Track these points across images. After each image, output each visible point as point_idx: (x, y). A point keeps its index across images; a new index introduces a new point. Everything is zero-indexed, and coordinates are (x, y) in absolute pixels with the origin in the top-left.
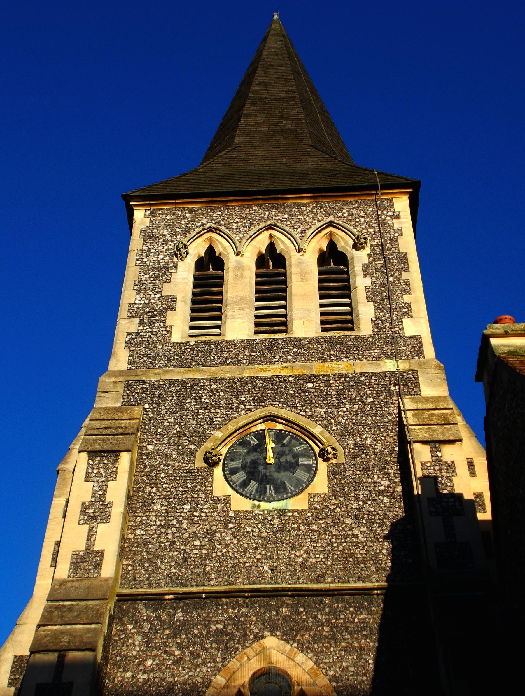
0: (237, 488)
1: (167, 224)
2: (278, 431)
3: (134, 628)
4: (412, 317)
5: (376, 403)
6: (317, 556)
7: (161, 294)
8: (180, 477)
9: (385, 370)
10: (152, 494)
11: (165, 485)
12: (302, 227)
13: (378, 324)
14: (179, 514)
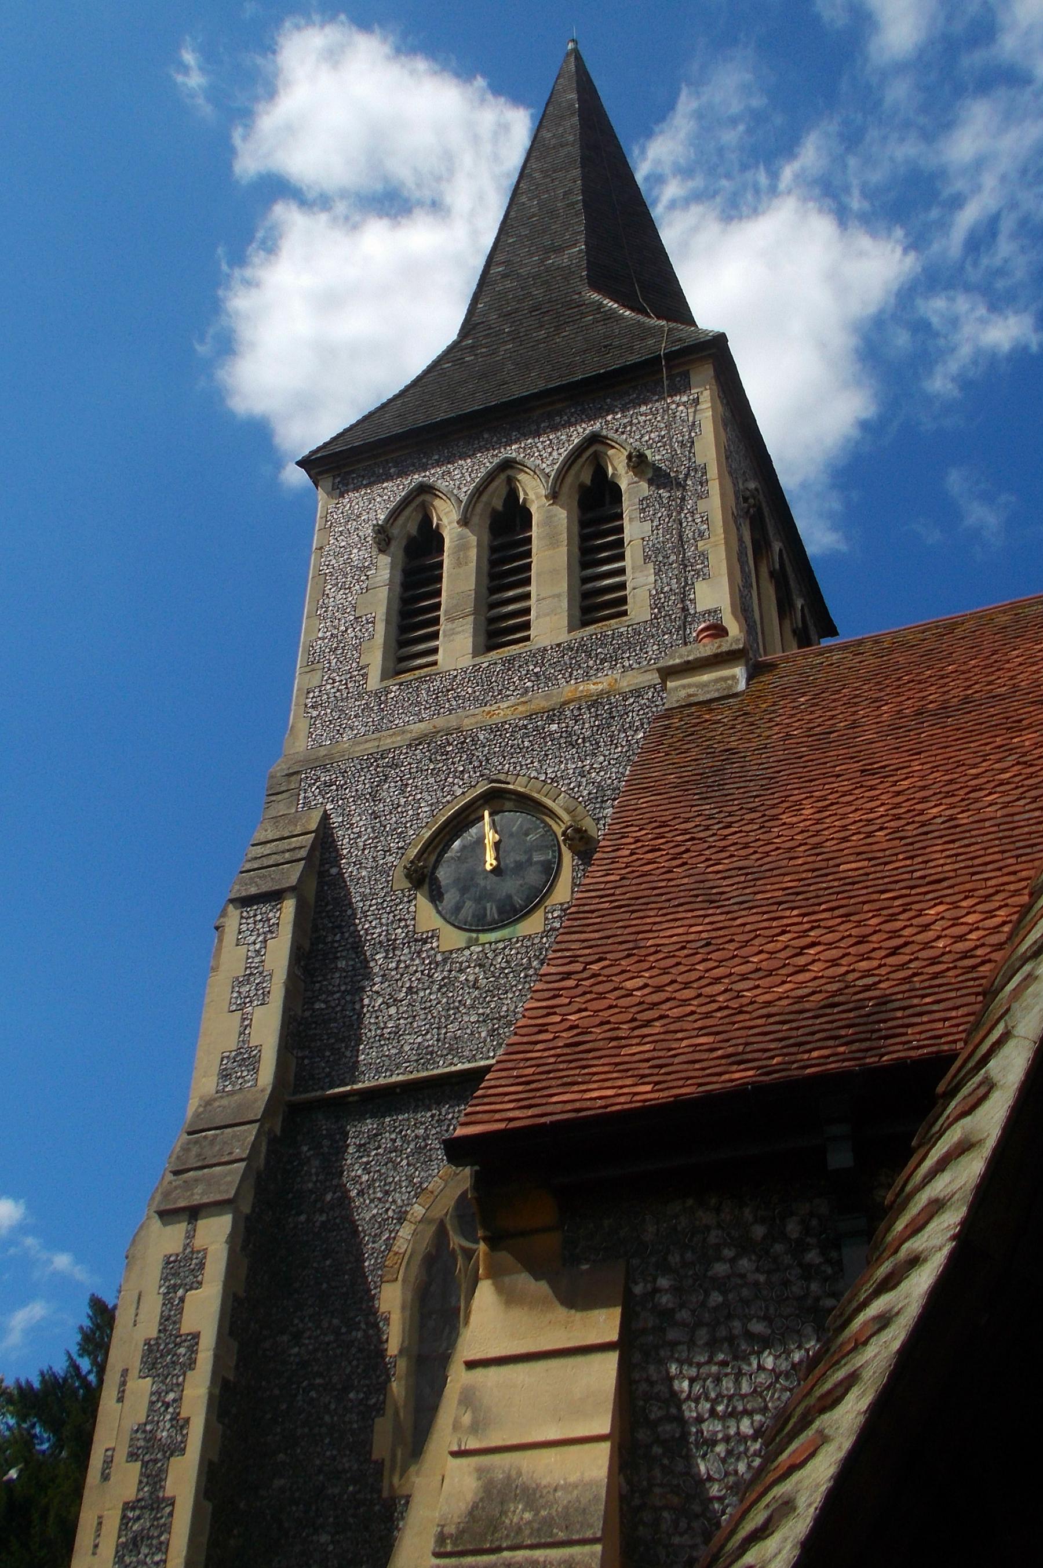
0: (448, 917)
3: (309, 1149)
10: (336, 945)
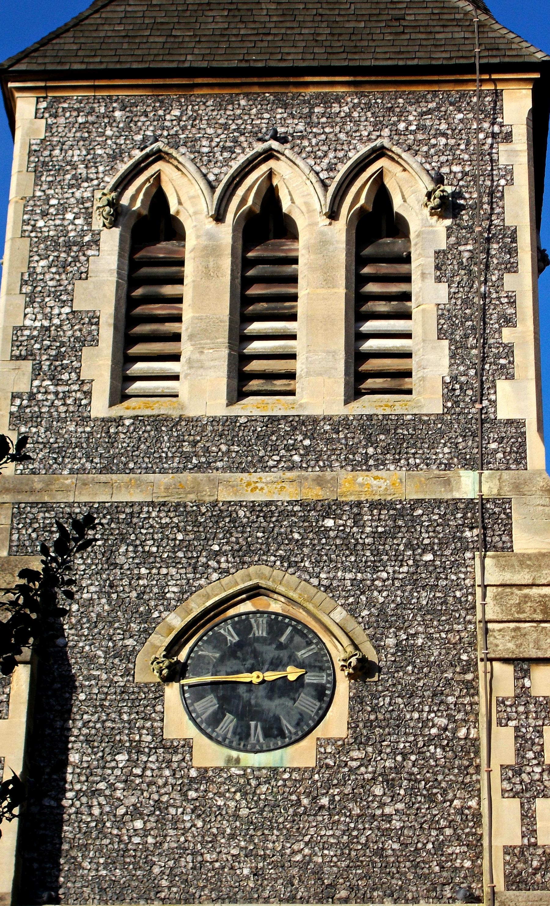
0: (203, 726)
1: (78, 134)
2: (273, 617)
4: (512, 377)
5: (438, 563)
6: (326, 852)
7: (72, 307)
8: (111, 700)
9: (457, 495)
11: (85, 717)
12: (331, 155)
13: (455, 390)
14: (109, 771)
